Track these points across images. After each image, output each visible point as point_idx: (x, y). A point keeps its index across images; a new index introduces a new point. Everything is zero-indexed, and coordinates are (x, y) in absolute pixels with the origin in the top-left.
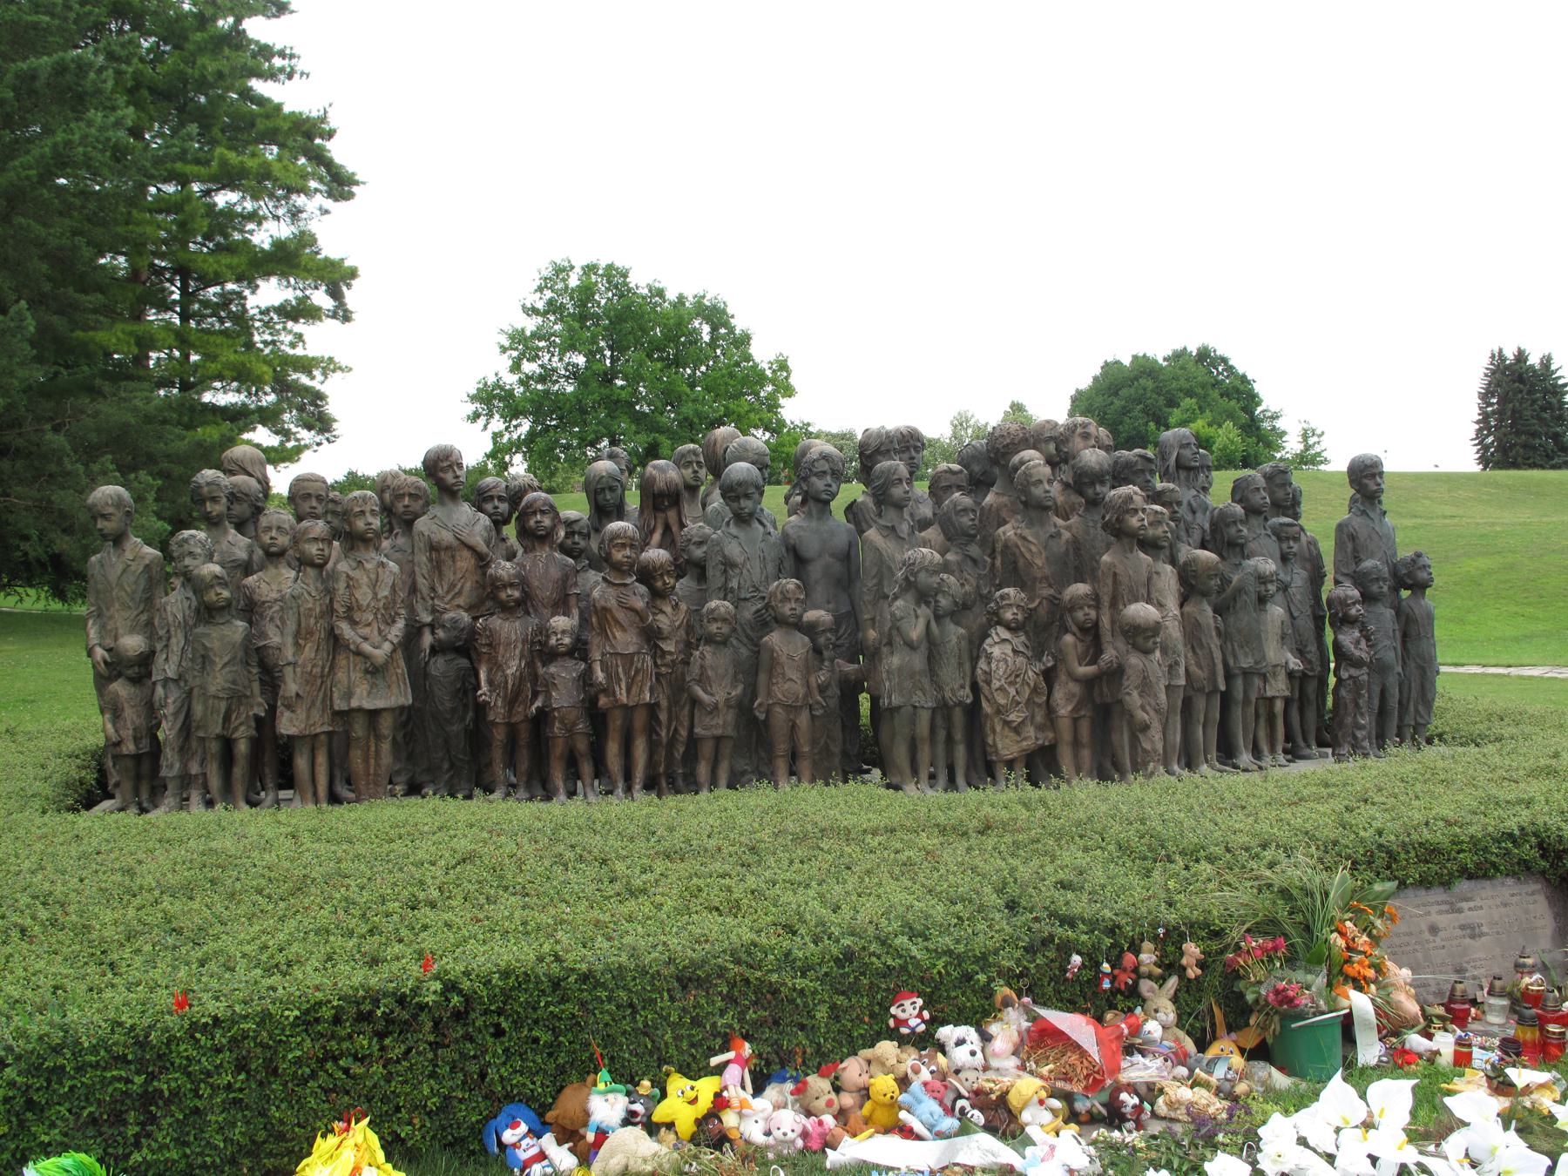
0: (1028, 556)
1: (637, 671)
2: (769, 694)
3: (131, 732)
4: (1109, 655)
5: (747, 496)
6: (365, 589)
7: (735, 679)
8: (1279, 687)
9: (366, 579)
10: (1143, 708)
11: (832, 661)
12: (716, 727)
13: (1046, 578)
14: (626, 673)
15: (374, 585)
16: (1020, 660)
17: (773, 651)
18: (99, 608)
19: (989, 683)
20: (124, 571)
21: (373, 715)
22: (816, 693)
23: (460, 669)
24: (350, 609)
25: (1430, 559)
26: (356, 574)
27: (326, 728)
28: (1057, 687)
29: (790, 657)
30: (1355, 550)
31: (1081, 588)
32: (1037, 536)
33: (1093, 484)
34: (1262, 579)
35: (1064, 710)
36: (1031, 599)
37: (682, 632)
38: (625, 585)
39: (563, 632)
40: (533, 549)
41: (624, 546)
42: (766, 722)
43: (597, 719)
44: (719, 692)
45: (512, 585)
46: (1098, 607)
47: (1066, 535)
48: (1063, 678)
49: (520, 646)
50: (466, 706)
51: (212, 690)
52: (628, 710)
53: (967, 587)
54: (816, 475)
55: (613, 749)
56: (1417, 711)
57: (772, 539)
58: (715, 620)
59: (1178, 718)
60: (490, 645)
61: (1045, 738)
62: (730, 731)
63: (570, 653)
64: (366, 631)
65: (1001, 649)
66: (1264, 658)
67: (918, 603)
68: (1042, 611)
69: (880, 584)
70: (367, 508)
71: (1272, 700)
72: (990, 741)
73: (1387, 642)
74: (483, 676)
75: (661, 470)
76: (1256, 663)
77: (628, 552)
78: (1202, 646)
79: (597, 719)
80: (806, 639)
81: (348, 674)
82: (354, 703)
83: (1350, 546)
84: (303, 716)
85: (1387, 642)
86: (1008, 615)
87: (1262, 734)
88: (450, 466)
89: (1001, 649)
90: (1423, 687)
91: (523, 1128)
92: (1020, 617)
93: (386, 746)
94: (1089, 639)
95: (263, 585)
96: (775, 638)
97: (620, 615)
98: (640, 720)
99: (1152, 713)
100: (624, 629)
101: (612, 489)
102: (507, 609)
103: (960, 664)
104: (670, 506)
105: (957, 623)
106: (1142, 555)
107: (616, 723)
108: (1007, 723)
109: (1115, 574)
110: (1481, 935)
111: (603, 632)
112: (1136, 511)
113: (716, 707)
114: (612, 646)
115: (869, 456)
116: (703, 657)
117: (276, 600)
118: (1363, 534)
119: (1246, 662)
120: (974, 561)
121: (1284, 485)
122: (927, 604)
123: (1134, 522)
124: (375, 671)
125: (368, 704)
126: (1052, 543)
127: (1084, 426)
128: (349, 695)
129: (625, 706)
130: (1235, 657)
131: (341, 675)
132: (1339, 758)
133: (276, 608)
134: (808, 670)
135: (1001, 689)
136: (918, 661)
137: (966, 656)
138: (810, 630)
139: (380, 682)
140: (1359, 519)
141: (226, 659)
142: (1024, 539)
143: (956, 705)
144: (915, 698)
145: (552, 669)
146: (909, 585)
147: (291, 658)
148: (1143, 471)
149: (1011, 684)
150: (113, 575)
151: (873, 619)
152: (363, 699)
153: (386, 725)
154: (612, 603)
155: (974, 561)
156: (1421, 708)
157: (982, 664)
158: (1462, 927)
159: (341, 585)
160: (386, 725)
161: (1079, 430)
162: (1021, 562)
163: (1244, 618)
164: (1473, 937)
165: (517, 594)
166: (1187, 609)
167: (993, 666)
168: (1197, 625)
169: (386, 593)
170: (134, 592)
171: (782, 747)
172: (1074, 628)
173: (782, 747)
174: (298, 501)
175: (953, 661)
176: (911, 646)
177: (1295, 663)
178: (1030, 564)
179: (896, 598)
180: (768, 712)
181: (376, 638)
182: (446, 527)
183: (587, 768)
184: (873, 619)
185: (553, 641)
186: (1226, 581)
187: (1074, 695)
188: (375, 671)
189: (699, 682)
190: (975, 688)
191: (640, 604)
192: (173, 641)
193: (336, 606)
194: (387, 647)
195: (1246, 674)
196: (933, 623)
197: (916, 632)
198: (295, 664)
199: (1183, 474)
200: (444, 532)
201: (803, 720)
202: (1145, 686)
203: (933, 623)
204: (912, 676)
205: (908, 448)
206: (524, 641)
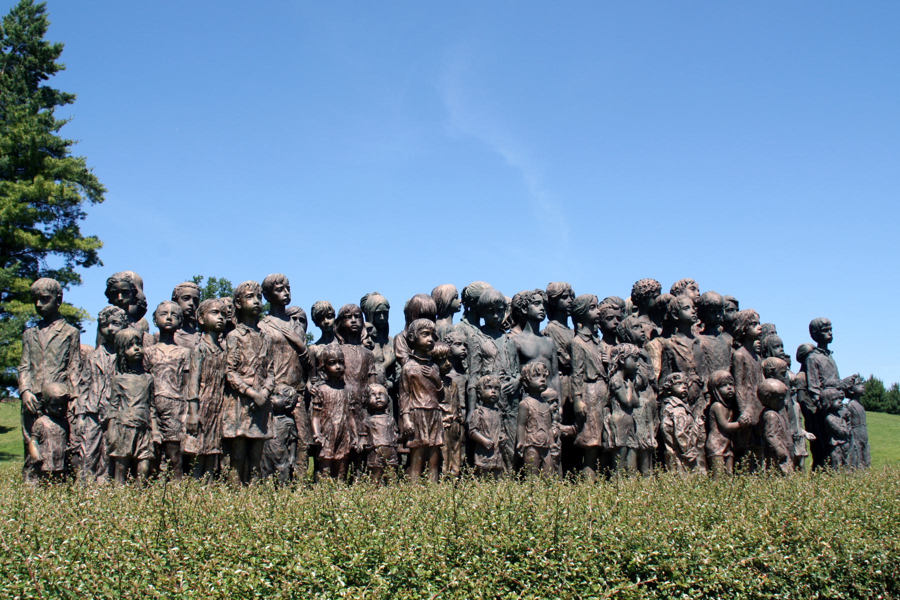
0: (682, 354)
1: (435, 422)
3: (51, 454)
6: (250, 350)
13: (694, 368)
14: (429, 423)
18: (32, 364)
20: (53, 339)
23: (288, 425)
26: (245, 339)
29: (541, 415)
30: (820, 374)
35: (719, 450)
39: (380, 393)
41: (427, 334)
46: (735, 385)
51: (126, 421)
58: (490, 387)
60: (320, 404)
64: (251, 380)
67: (625, 379)
69: (584, 372)
84: (202, 440)
86: (680, 389)
95: (159, 352)
100: (426, 392)
103: (647, 422)
108: (685, 460)
109: (745, 364)
114: (419, 403)
116: (481, 413)
117: (168, 364)
126: (695, 346)
133: (168, 369)
141: (137, 399)
142: (678, 343)
145: (372, 419)
150: (44, 341)
151: (581, 395)
157: (666, 421)
161: (689, 285)
162: (678, 358)
167: (675, 421)
170: (59, 354)
174: (180, 300)
184: (581, 395)
185: (373, 399)
187: (724, 442)
189: (478, 429)
192: (95, 385)
198: (197, 400)
206: (346, 402)
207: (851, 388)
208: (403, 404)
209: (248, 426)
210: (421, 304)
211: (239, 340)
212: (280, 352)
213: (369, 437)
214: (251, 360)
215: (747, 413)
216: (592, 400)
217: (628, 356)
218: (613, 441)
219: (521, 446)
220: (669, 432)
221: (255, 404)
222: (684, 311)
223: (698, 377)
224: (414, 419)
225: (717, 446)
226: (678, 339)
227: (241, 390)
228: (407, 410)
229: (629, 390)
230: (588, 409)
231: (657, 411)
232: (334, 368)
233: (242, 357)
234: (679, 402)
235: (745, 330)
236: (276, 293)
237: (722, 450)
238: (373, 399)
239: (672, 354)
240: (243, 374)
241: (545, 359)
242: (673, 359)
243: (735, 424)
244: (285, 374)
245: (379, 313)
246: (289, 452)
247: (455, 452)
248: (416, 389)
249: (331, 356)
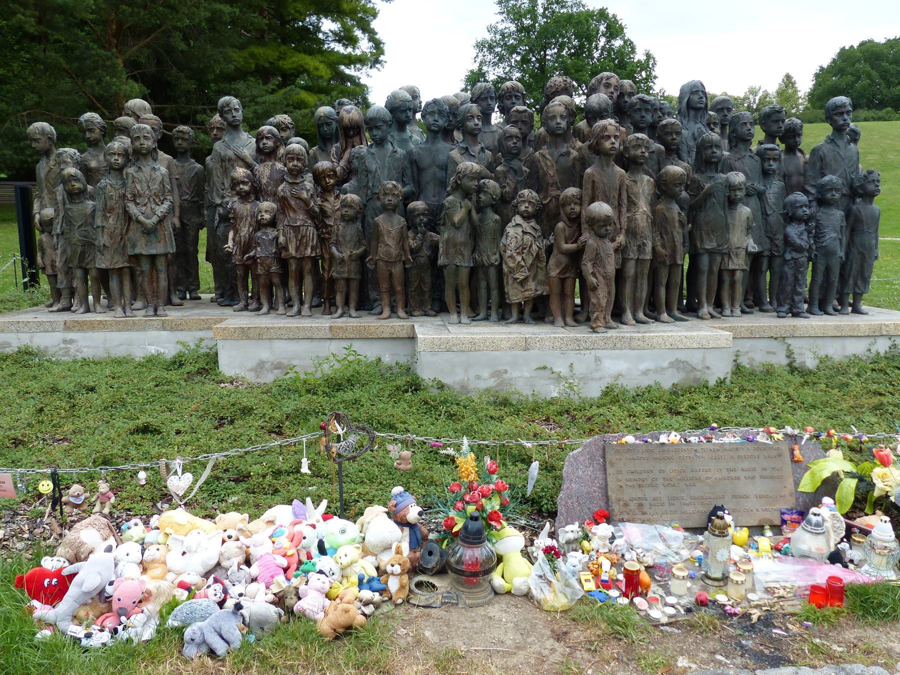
1: (303, 237)
5: (377, 128)
7: (359, 243)
8: (739, 263)
10: (594, 274)
11: (424, 234)
12: (343, 272)
16: (527, 237)
19: (505, 252)
21: (153, 258)
24: (134, 196)
25: (884, 176)
27: (127, 265)
29: (390, 232)
30: (821, 168)
31: (572, 191)
32: (551, 155)
34: (731, 187)
35: (554, 273)
36: (545, 198)
39: (266, 211)
42: (375, 271)
43: (284, 263)
45: (243, 183)
47: (574, 153)
48: (555, 251)
49: (249, 218)
52: (300, 260)
53: (507, 189)
55: (292, 283)
56: (856, 284)
57: (398, 156)
59: (645, 282)
61: (542, 290)
62: (353, 276)
65: (518, 231)
66: (727, 241)
67: (463, 198)
68: (552, 206)
71: (733, 272)
73: (834, 235)
75: (348, 112)
76: (718, 246)
78: (667, 233)
79: (284, 263)
80: (403, 219)
81: (134, 233)
82: (137, 251)
83: (818, 164)
85: (834, 235)
87: (726, 295)
88: (230, 110)
89: (518, 231)
90: (862, 266)
92: (530, 209)
94: (575, 226)
96: (380, 219)
98: (308, 266)
99: (601, 278)
100: (295, 211)
101: (328, 124)
102: (244, 197)
104: (355, 135)
105: (496, 212)
106: (618, 169)
107: (293, 266)
109: (593, 182)
111: (284, 213)
112: (609, 137)
113: (342, 261)
118: (830, 157)
119: (710, 245)
120: (515, 171)
121: (777, 121)
122: (470, 200)
123: (607, 145)
126: (562, 159)
127: (608, 78)
128: (134, 246)
129: (294, 258)
130: (702, 241)
132: (594, 330)
134: (402, 238)
135: (511, 257)
136: (461, 237)
138: (409, 215)
139: (153, 238)
140: (828, 146)
141: (80, 223)
142: (544, 156)
146: (457, 187)
147: (100, 224)
148: (640, 110)
149: (518, 254)
152: (142, 248)
153: (161, 264)
155: (515, 171)
156: (859, 282)
157: (503, 240)
159: (130, 181)
160: (161, 264)
161: (604, 81)
162: (541, 171)
163: (713, 213)
166: (659, 207)
168: (665, 218)
171: (384, 286)
172: (565, 218)
173: (384, 286)
176: (453, 224)
177: (753, 246)
178: (545, 174)
183: (279, 293)
186: (700, 187)
188: (149, 232)
191: (305, 195)
195: (711, 253)
196: (474, 213)
197: (458, 216)
199: (692, 113)
201: (397, 270)
202: (597, 260)
203: (474, 213)
204: (455, 246)
205: (511, 97)
207: (862, 186)
217: (464, 176)
219: (370, 260)
237: (558, 271)
239: (537, 167)
240: (138, 204)
242: (538, 172)
243: (574, 245)
245: (322, 124)
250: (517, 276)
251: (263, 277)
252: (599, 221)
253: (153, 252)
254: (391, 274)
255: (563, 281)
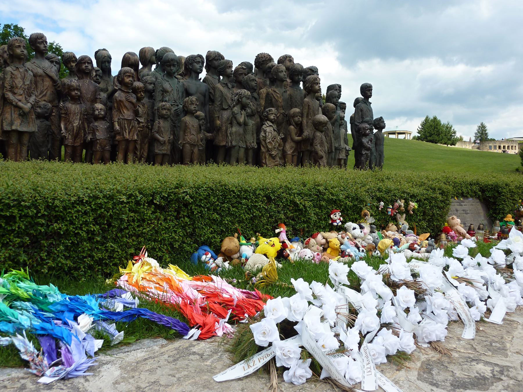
0: (276, 98)
1: (132, 127)
2: (184, 139)
4: (306, 133)
5: (174, 65)
6: (19, 79)
9: (19, 76)
12: (164, 150)
13: (282, 106)
15: (23, 78)
17: (186, 123)
19: (265, 141)
21: (20, 134)
22: (200, 141)
23: (47, 125)
24: (12, 87)
26: (15, 73)
28: (287, 144)
29: (193, 126)
30: (362, 115)
33: (298, 75)
35: (289, 152)
37: (146, 115)
38: (128, 92)
39: (101, 109)
40: (82, 78)
41: (129, 76)
44: (165, 137)
46: (302, 117)
48: (289, 140)
49: (79, 115)
50: (48, 141)
52: (127, 141)
54: (196, 62)
58: (165, 109)
60: (66, 114)
63: (103, 118)
64: (20, 97)
65: (269, 129)
69: (221, 104)
70: (22, 45)
72: (264, 161)
74: (62, 126)
77: (131, 79)
78: (328, 136)
82: (14, 128)
83: (360, 113)
86: (272, 117)
88: (42, 42)
89: (269, 129)
91: (209, 255)
93: (25, 149)
96: (187, 119)
97: (127, 104)
98: (131, 147)
100: (128, 110)
103: (253, 134)
107: (122, 146)
108: (271, 155)
109: (309, 105)
110: (468, 213)
115: (211, 60)
116: (159, 123)
122: (245, 110)
124: (24, 115)
125: (20, 129)
126: (284, 94)
128: (11, 124)
131: (8, 116)
137: (255, 132)
142: (275, 91)
143: (251, 148)
144: (240, 144)
145: (96, 124)
149: (273, 141)
154: (124, 99)
157: (262, 134)
158: (463, 210)
159: (8, 77)
160: (26, 139)
161: (288, 59)
162: (274, 100)
164: (466, 214)
165: (79, 93)
167: (267, 134)
169: (28, 83)
172: (294, 124)
175: (251, 133)
176: (239, 124)
178: (277, 101)
179: (234, 107)
180: (183, 146)
181: (25, 101)
182: (39, 67)
184: (219, 117)
185: (97, 112)
187: (293, 147)
189: (157, 132)
190: (259, 143)
193: (6, 85)
194: (29, 105)
200: (39, 69)
201: (196, 150)
202: (322, 144)
204: (240, 135)
206: (81, 113)
208: (115, 116)
209: (19, 124)
210: (130, 58)
211: (12, 73)
212: (41, 82)
213: (94, 134)
214: (20, 86)
215: (307, 133)
216: (224, 120)
218: (231, 143)
219: (181, 143)
220: (263, 140)
221: (23, 112)
222: (279, 74)
223: (284, 111)
224: (120, 125)
225: (289, 149)
226: (275, 90)
227: (14, 103)
228: (116, 119)
229: (243, 116)
230: (222, 125)
231: (259, 129)
232: (73, 93)
233: (14, 84)
234: (271, 124)
235: (311, 86)
236: (38, 45)
238: (97, 112)
239: (271, 97)
241: (200, 95)
242: (271, 100)
243: (300, 138)
244: (45, 95)
245: (105, 62)
246: (48, 141)
247: (145, 144)
248: (122, 108)
249: (72, 86)
250: (273, 153)
251: (99, 153)
252: (324, 123)
253: (24, 129)
254: (192, 153)
255: (293, 156)
